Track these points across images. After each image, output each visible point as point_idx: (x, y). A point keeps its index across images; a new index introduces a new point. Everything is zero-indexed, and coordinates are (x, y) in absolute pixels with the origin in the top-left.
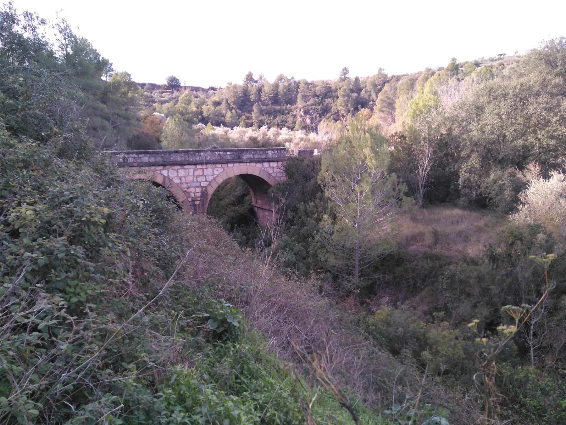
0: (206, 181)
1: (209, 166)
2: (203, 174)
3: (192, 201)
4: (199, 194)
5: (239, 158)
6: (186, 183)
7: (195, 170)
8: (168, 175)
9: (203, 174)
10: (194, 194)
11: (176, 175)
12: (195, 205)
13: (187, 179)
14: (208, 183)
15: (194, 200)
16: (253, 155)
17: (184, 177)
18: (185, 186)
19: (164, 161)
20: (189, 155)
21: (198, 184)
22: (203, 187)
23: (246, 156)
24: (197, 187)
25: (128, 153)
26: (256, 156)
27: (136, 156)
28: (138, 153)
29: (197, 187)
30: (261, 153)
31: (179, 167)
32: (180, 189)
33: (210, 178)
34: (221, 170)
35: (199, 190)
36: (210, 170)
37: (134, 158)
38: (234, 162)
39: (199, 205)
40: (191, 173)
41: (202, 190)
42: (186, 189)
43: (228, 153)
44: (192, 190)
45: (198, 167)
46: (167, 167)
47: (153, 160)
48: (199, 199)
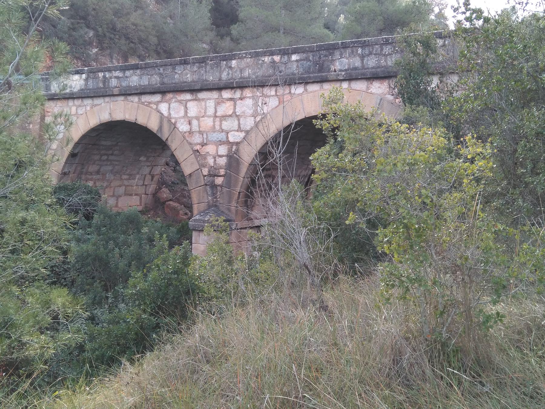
0: (239, 130)
1: (248, 92)
2: (234, 112)
3: (210, 175)
4: (223, 161)
5: (321, 70)
6: (200, 132)
7: (218, 103)
8: (170, 114)
9: (234, 112)
10: (215, 158)
11: (182, 113)
12: (214, 186)
13: (202, 124)
14: (242, 135)
15: (213, 174)
16: (362, 57)
17: (197, 118)
18: (197, 139)
19: (163, 83)
20: (208, 67)
21: (222, 136)
22: (232, 144)
23: (341, 63)
24: (221, 143)
25: (109, 70)
26: (371, 62)
27: (120, 74)
28: (124, 69)
29: (221, 143)
30: (387, 50)
31: (188, 96)
32: (188, 147)
33: (248, 123)
34: (273, 102)
35: (223, 150)
36: (249, 102)
37: (117, 78)
38: (305, 82)
39: (221, 186)
40: (211, 111)
41: (230, 150)
42: (198, 147)
43: (294, 57)
44: (211, 149)
45: (226, 94)
46: (169, 96)
47: (145, 81)
48: (222, 172)
